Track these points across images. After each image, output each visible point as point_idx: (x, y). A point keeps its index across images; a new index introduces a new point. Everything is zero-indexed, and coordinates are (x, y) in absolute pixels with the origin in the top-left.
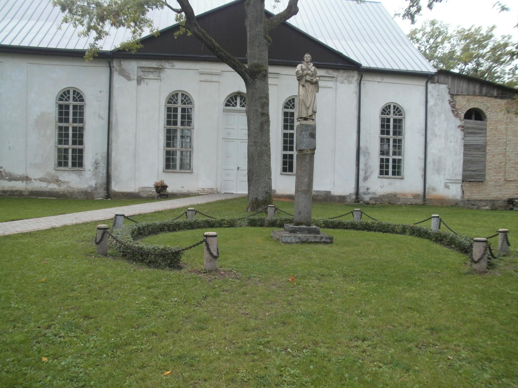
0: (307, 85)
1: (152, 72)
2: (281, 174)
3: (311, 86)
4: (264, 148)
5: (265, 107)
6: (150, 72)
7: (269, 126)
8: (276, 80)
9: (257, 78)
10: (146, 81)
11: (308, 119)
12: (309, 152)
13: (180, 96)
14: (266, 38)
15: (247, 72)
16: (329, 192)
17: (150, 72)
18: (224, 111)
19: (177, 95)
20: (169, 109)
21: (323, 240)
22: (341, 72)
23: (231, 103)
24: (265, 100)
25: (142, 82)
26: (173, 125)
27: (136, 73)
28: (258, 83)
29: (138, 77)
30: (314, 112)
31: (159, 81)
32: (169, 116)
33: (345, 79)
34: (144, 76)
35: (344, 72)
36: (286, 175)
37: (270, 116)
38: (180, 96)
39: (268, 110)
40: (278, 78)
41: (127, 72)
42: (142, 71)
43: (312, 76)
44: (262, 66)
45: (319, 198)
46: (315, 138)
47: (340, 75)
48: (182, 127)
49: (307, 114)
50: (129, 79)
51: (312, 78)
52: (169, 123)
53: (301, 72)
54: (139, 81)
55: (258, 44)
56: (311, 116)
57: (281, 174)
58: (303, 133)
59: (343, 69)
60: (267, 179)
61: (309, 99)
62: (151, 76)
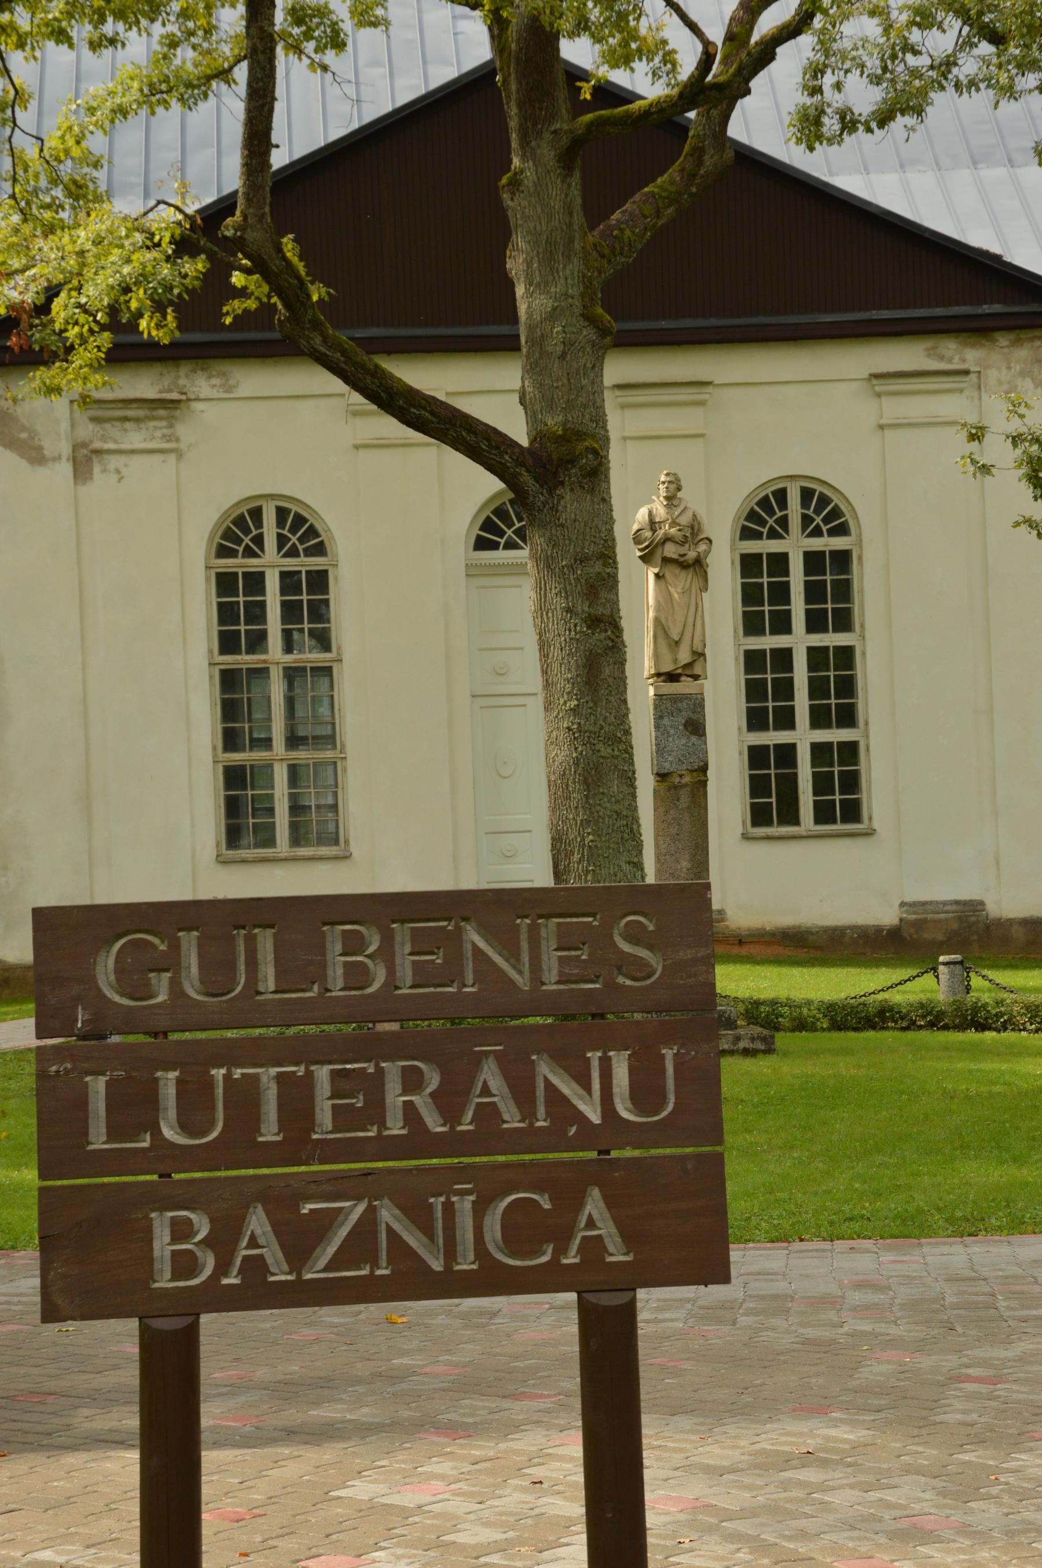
0: (670, 572)
1: (138, 420)
2: (746, 837)
3: (683, 574)
4: (605, 751)
5: (603, 594)
6: (126, 419)
7: (622, 663)
8: (699, 411)
9: (562, 483)
10: (114, 462)
11: (680, 675)
12: (687, 779)
13: (269, 518)
14: (589, 318)
15: (522, 465)
16: (975, 906)
17: (126, 419)
18: (472, 571)
19: (256, 513)
20: (225, 583)
21: (742, 1045)
22: (1003, 340)
23: (501, 533)
24: (598, 567)
25: (97, 469)
26: (248, 653)
27: (64, 426)
28: (571, 504)
29: (75, 448)
30: (699, 655)
31: (172, 458)
32: (226, 613)
33: (1023, 374)
34: (104, 439)
35: (1016, 343)
36: (768, 838)
37: (624, 623)
38: (269, 518)
39: (616, 602)
40: (702, 403)
41: (24, 429)
42: (94, 420)
43: (682, 544)
44: (580, 435)
45: (928, 936)
46: (704, 734)
47: (995, 357)
48: (289, 658)
49: (675, 661)
50: (36, 456)
51: (682, 550)
52: (228, 643)
53: (648, 534)
54: (84, 461)
55: (560, 349)
56: (689, 665)
57: (746, 837)
58: (666, 721)
59: (1009, 329)
60: (626, 868)
61: (679, 618)
62: (135, 438)
